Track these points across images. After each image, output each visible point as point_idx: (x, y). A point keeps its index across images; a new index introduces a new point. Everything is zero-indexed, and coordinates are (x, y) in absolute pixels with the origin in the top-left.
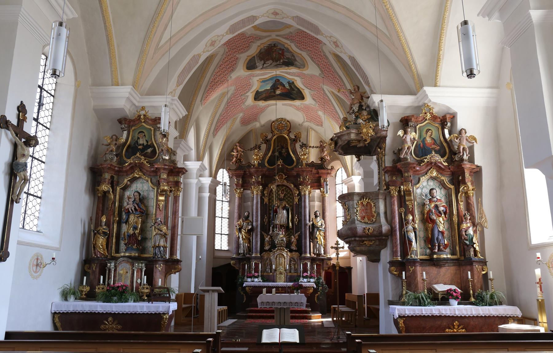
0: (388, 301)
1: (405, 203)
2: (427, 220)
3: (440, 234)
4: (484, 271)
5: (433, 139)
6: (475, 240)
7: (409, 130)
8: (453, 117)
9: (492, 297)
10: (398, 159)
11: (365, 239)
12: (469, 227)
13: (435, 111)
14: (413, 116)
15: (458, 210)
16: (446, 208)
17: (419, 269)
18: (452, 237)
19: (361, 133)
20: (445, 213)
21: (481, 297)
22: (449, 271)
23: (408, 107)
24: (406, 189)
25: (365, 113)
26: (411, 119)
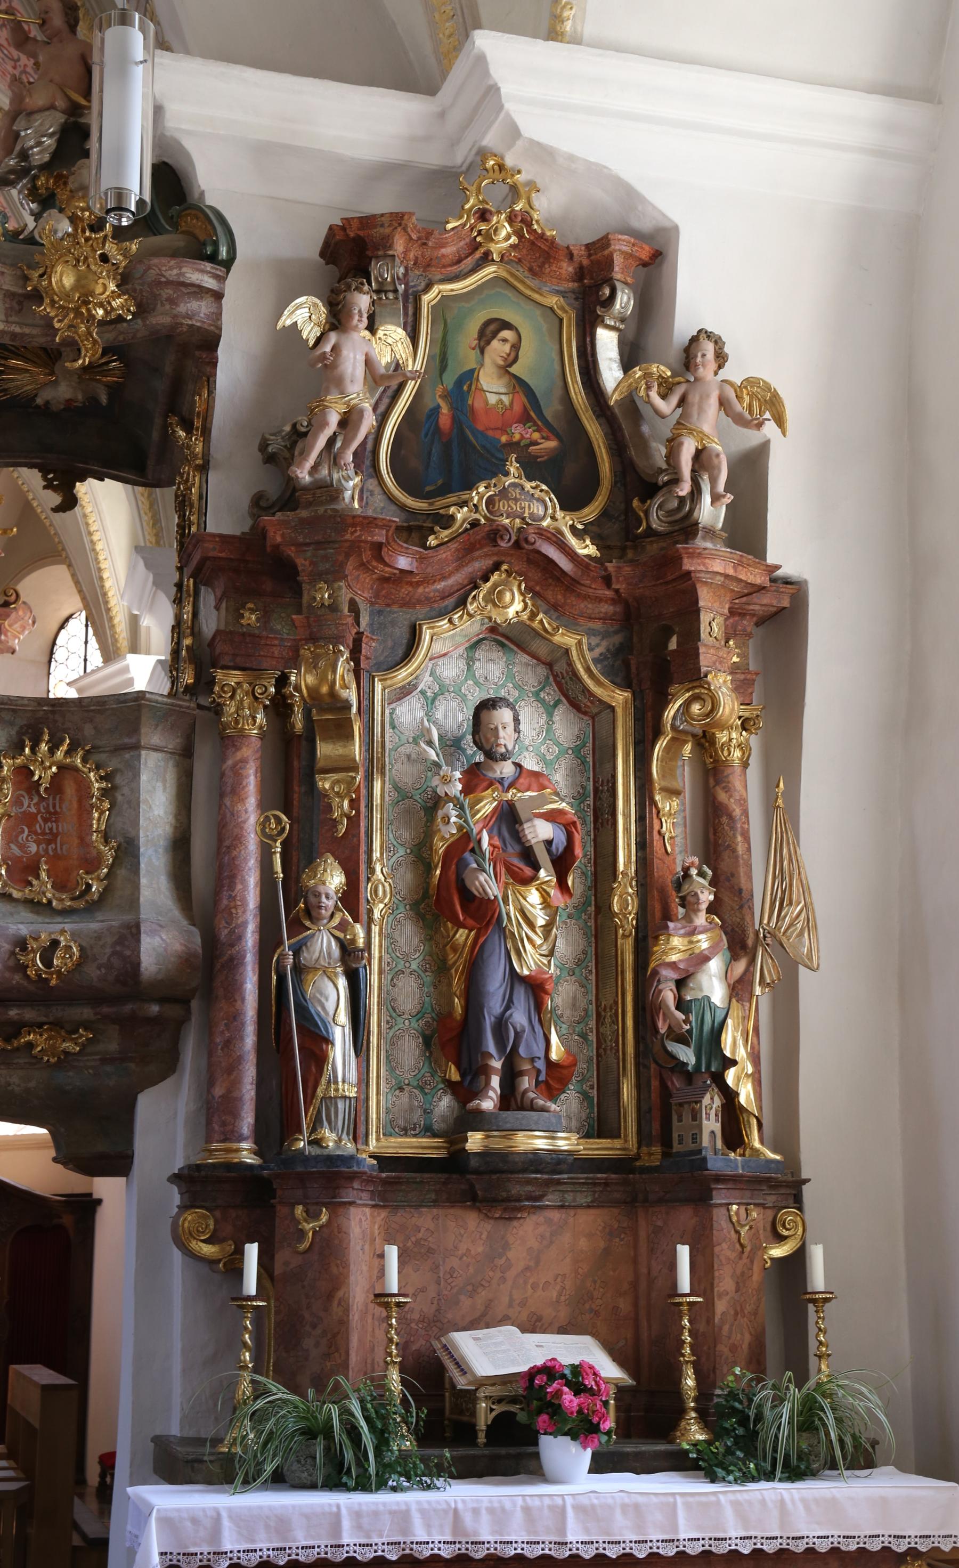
0: (160, 1442)
1: (312, 785)
2: (448, 902)
3: (521, 995)
4: (780, 1239)
5: (519, 384)
6: (732, 1042)
7: (363, 301)
8: (655, 257)
9: (808, 1419)
10: (284, 498)
11: (29, 1014)
12: (704, 959)
13: (547, 206)
14: (398, 219)
15: (643, 844)
16: (569, 828)
17: (361, 1221)
18: (604, 1013)
19: (37, 296)
20: (562, 863)
21: (744, 1420)
22: (566, 1238)
23: (383, 171)
24: (314, 692)
26: (386, 243)
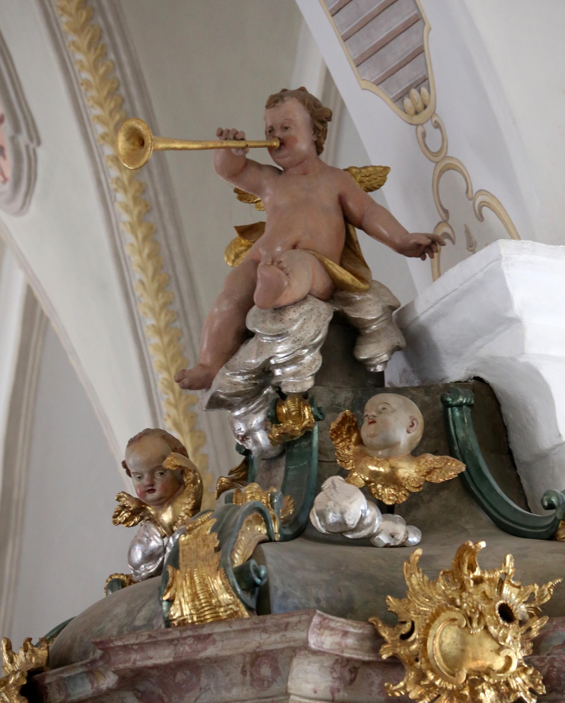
25: (401, 422)
